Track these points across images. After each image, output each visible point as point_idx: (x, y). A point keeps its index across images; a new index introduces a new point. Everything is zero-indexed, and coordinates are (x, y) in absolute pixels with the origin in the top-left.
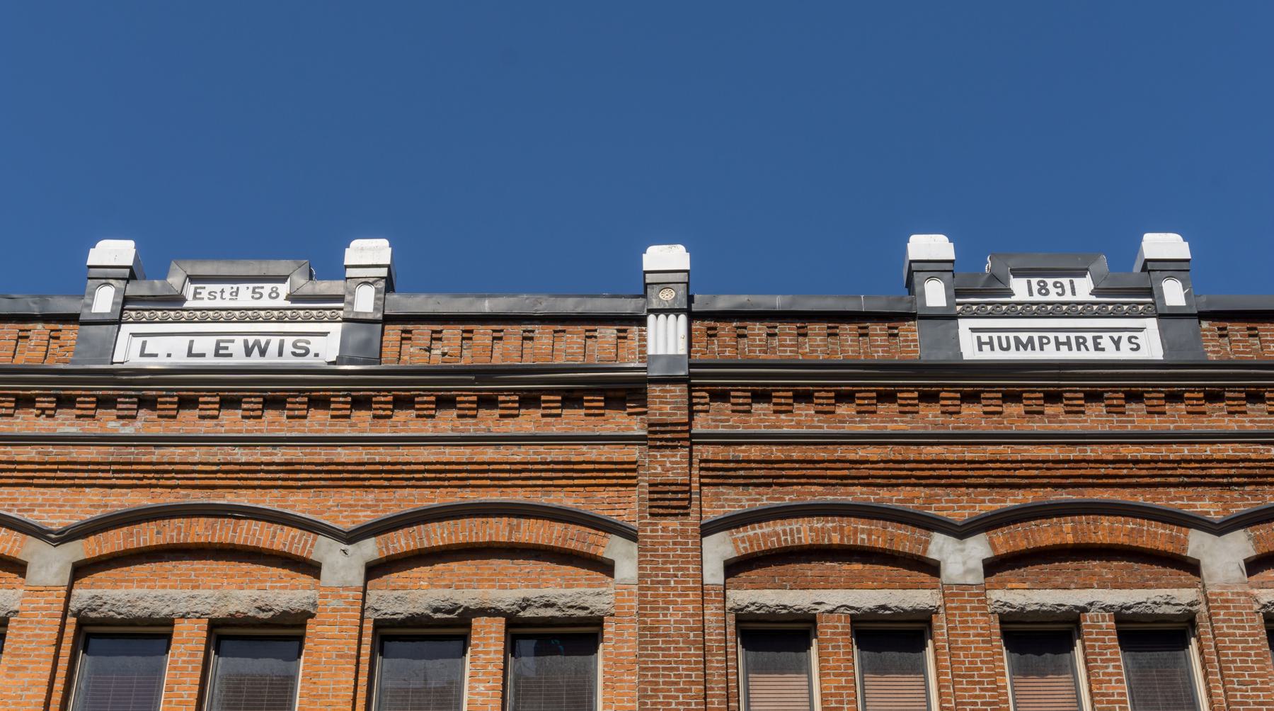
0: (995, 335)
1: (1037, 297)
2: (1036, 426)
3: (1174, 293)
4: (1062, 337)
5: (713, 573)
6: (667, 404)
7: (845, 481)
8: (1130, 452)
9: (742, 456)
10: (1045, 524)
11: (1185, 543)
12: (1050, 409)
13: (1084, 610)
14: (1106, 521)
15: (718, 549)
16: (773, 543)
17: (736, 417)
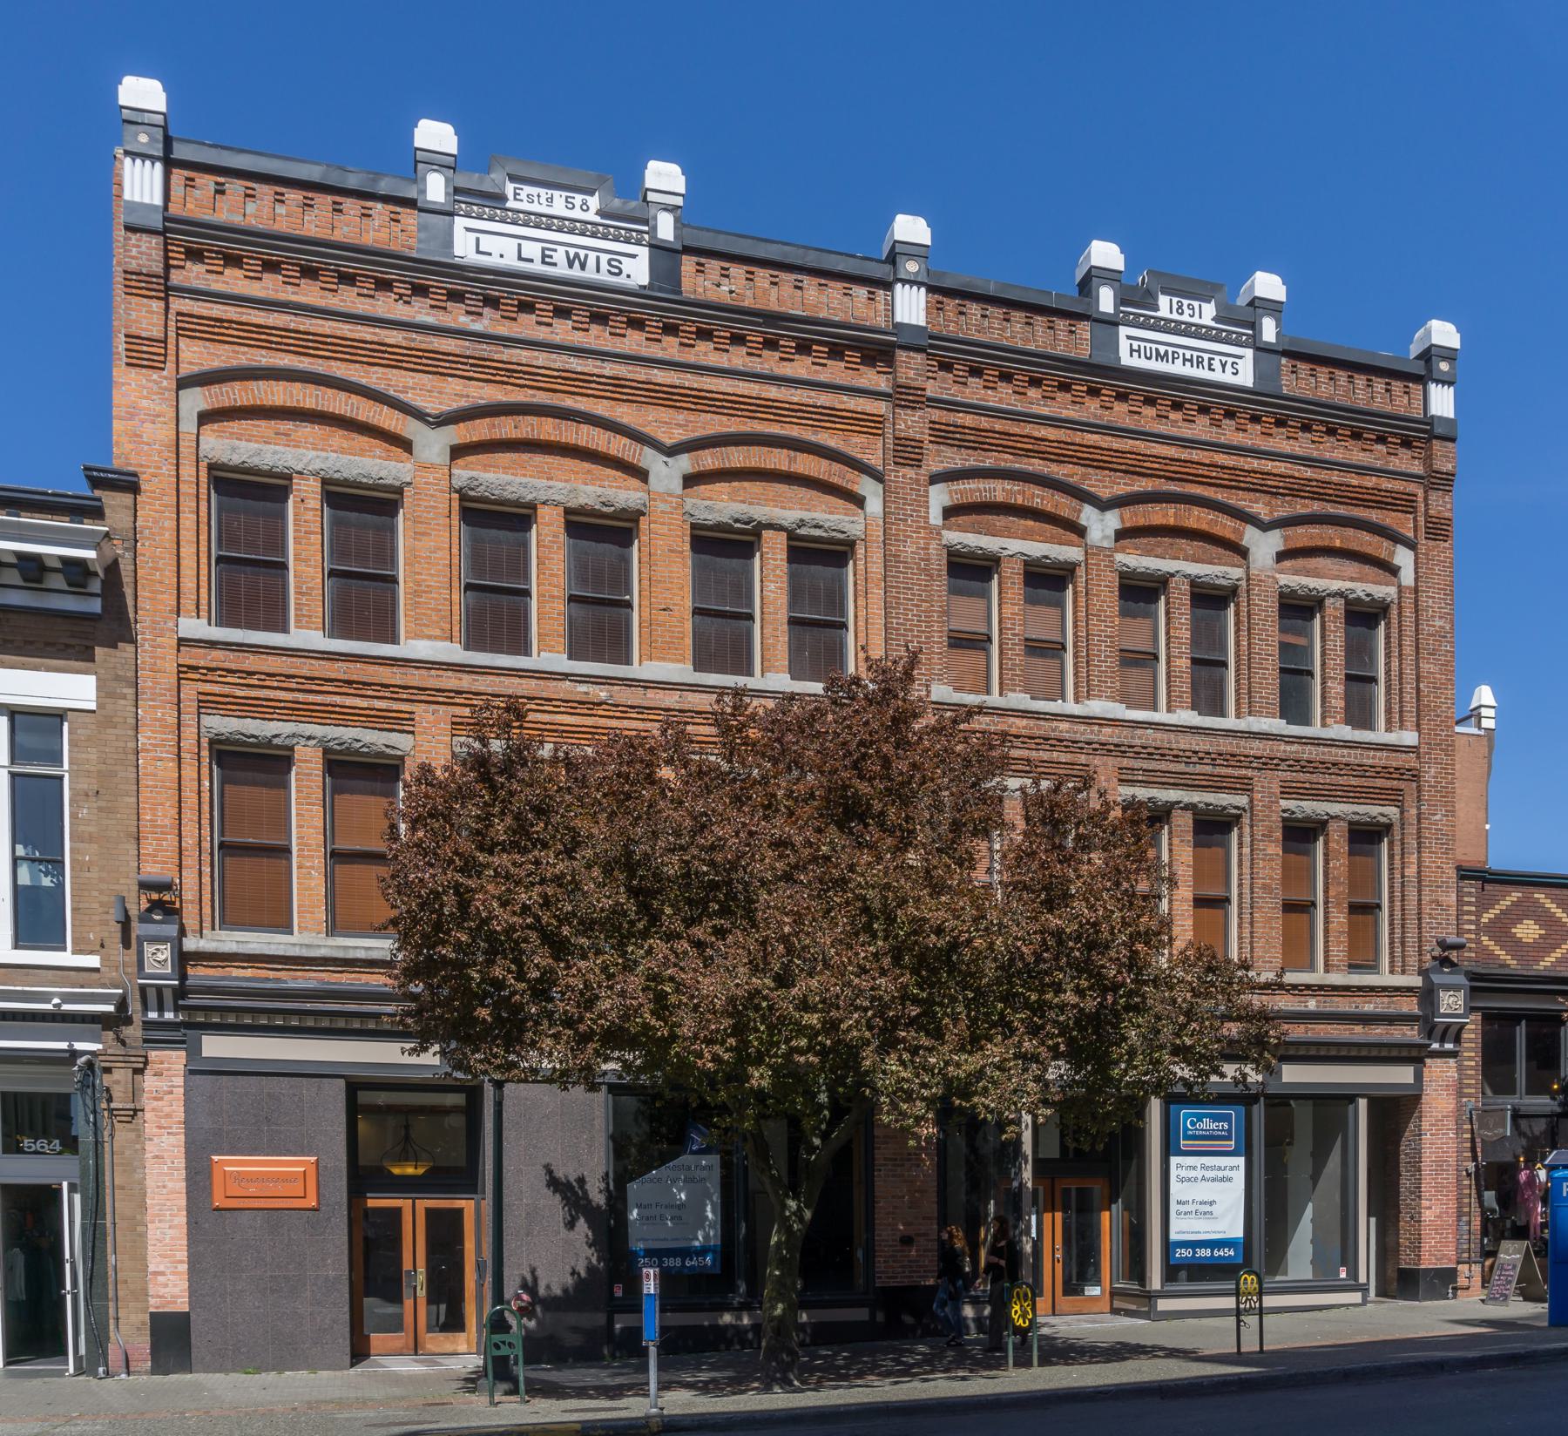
0: (1142, 344)
1: (1175, 316)
2: (1162, 428)
3: (1269, 331)
4: (1188, 354)
5: (935, 517)
6: (911, 367)
7: (1028, 453)
8: (1221, 459)
9: (960, 422)
10: (1158, 507)
11: (1242, 535)
12: (1173, 416)
13: (1173, 575)
14: (1196, 511)
15: (939, 497)
16: (976, 498)
17: (956, 387)
